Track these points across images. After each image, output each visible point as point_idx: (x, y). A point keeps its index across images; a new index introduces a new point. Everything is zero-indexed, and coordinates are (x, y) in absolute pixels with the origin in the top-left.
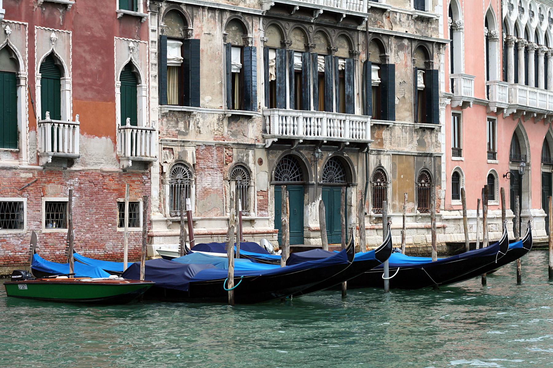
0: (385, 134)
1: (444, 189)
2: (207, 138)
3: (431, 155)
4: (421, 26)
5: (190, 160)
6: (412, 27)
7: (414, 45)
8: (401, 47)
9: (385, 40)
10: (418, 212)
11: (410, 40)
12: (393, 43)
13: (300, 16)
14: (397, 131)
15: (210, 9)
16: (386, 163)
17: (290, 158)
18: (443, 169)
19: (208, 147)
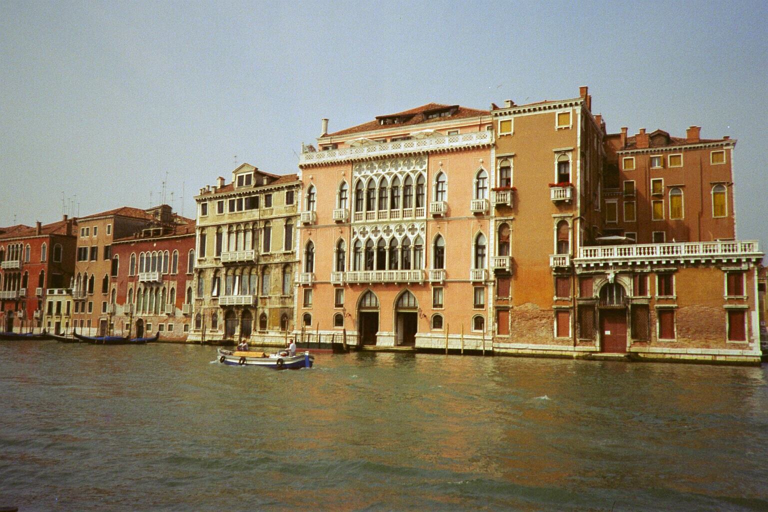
0: (268, 301)
1: (297, 321)
2: (206, 306)
3: (288, 308)
4: (287, 257)
5: (202, 313)
6: (283, 258)
7: (283, 265)
8: (277, 267)
9: (269, 266)
10: (280, 331)
11: (282, 263)
12: (273, 266)
13: (234, 264)
14: (273, 299)
15: (211, 268)
16: (267, 312)
17: (229, 311)
18: (295, 313)
19: (207, 309)
